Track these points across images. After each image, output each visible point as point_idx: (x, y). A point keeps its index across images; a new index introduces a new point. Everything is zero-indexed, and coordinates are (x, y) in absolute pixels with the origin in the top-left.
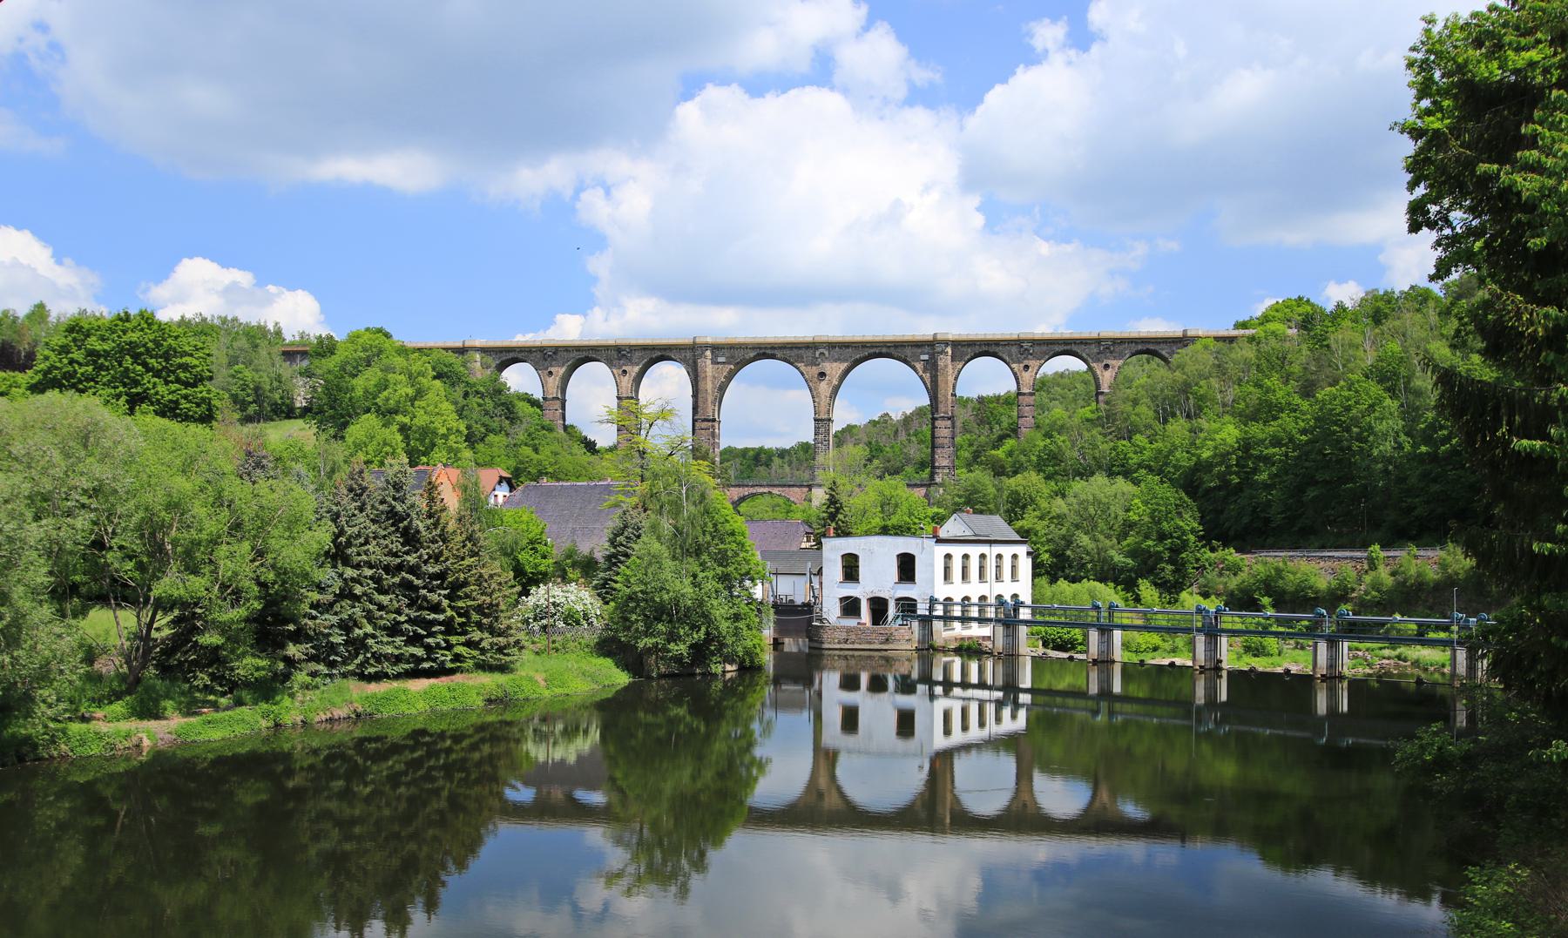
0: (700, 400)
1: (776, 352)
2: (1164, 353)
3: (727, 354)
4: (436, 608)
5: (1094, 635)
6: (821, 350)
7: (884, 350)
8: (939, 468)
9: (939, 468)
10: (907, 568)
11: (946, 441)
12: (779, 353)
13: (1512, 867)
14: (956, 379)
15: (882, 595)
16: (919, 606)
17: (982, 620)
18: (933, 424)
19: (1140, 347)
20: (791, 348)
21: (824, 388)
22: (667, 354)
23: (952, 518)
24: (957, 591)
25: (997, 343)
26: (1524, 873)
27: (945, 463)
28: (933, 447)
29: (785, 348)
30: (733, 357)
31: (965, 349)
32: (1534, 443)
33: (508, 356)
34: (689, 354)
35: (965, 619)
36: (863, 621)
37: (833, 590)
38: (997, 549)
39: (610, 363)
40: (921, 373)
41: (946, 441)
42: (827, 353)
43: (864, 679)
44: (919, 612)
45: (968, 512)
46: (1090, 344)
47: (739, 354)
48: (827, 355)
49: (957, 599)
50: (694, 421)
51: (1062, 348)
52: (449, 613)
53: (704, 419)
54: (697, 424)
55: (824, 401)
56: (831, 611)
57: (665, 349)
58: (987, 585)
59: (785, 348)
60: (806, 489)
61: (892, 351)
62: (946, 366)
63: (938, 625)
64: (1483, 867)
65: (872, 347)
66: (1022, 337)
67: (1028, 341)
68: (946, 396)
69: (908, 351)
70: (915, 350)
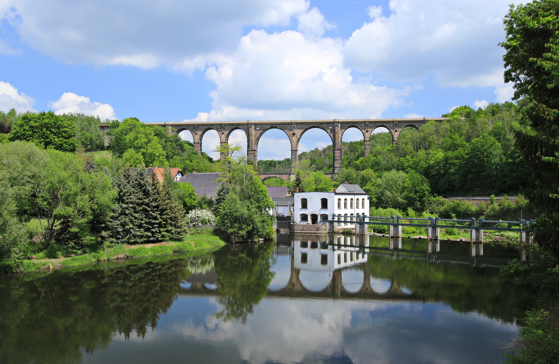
0: (250, 143)
1: (277, 126)
2: (417, 126)
3: (260, 127)
4: (155, 218)
5: (392, 228)
6: (294, 125)
7: (316, 125)
8: (336, 167)
9: (336, 167)
10: (324, 204)
11: (339, 158)
12: (278, 126)
13: (542, 311)
14: (342, 135)
15: (316, 213)
16: (329, 217)
17: (351, 222)
18: (334, 152)
19: (408, 124)
20: (283, 125)
21: (295, 139)
22: (238, 127)
23: (341, 185)
24: (342, 212)
25: (357, 122)
26: (547, 313)
27: (338, 166)
28: (334, 160)
29: (281, 124)
32: (550, 158)
33: (181, 128)
34: (246, 127)
35: (345, 222)
36: (309, 223)
37: (298, 211)
38: (357, 197)
39: (218, 130)
40: (329, 133)
41: (339, 158)
42: (295, 126)
43: (309, 243)
44: (329, 219)
45: (346, 183)
46: (390, 123)
47: (264, 127)
48: (296, 127)
49: (343, 215)
50: (248, 151)
51: (380, 124)
52: (160, 220)
53: (251, 150)
54: (249, 152)
55: (295, 143)
56: (297, 219)
57: (237, 125)
58: (353, 210)
59: (281, 124)
60: (288, 175)
61: (319, 125)
62: (338, 131)
63: (336, 224)
64: (531, 311)
65: (312, 124)
66: (366, 120)
67: (368, 122)
68: (338, 142)
69: (325, 126)
70: (327, 125)
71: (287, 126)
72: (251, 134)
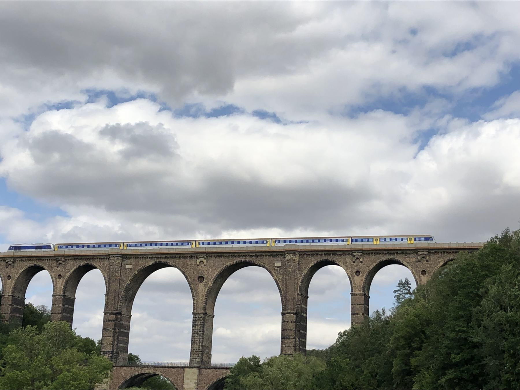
3: (134, 263)
6: (202, 259)
7: (248, 259)
25: (334, 252)
31: (309, 258)
34: (106, 263)
39: (50, 270)
42: (205, 261)
46: (410, 254)
48: (205, 261)
55: (202, 299)
60: (182, 369)
61: (254, 260)
65: (239, 256)
67: (359, 251)
69: (266, 260)
71: (188, 260)
72: (114, 279)
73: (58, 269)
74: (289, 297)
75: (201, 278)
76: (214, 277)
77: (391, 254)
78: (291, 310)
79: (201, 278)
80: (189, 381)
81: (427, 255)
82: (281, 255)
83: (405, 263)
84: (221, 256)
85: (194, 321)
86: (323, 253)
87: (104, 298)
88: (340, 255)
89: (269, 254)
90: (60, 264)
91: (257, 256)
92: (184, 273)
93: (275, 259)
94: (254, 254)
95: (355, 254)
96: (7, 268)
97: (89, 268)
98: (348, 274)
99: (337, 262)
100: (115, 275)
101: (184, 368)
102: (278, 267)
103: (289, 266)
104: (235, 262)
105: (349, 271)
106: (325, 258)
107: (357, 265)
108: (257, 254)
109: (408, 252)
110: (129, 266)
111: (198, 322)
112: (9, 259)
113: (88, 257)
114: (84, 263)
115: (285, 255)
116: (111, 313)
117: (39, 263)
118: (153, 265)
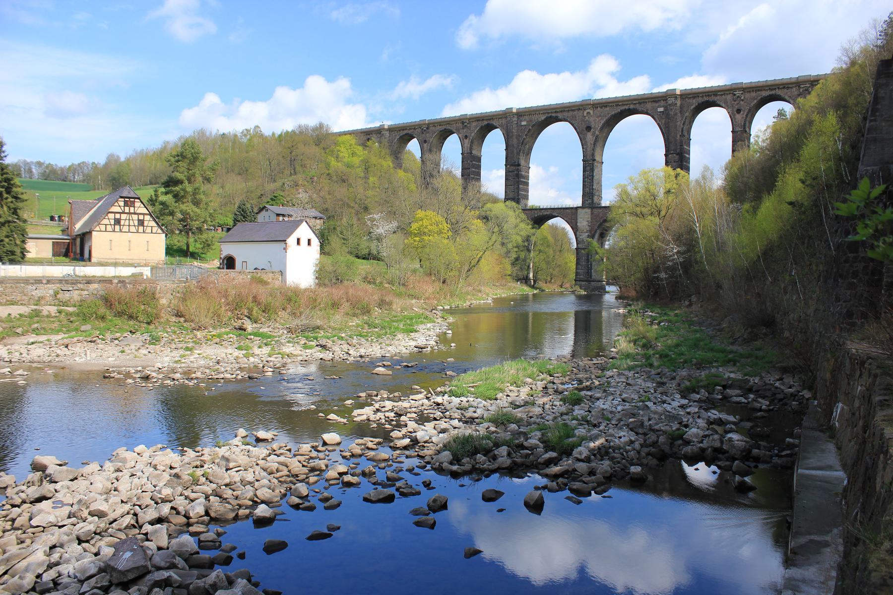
3: (527, 119)
6: (588, 111)
7: (632, 107)
20: (568, 111)
21: (589, 136)
29: (564, 111)
30: (531, 121)
42: (591, 112)
46: (792, 88)
48: (591, 112)
57: (490, 119)
62: (676, 114)
65: (623, 105)
69: (649, 106)
71: (576, 113)
73: (465, 130)
74: (672, 139)
75: (589, 128)
76: (600, 125)
77: (771, 90)
78: (674, 150)
79: (589, 128)
80: (582, 220)
81: (810, 87)
82: (663, 100)
83: (787, 97)
84: (606, 106)
85: (584, 168)
86: (704, 95)
87: (504, 153)
88: (722, 95)
89: (652, 100)
90: (466, 126)
91: (640, 103)
92: (573, 125)
93: (657, 105)
94: (637, 102)
95: (736, 93)
96: (423, 133)
97: (489, 128)
98: (728, 113)
99: (718, 102)
100: (512, 132)
101: (577, 208)
102: (660, 112)
103: (671, 110)
104: (619, 110)
105: (730, 110)
106: (706, 99)
107: (738, 104)
108: (640, 101)
109: (790, 86)
110: (524, 123)
111: (588, 168)
112: (424, 126)
113: (487, 118)
114: (486, 123)
115: (667, 99)
116: (512, 165)
117: (448, 127)
118: (546, 119)
